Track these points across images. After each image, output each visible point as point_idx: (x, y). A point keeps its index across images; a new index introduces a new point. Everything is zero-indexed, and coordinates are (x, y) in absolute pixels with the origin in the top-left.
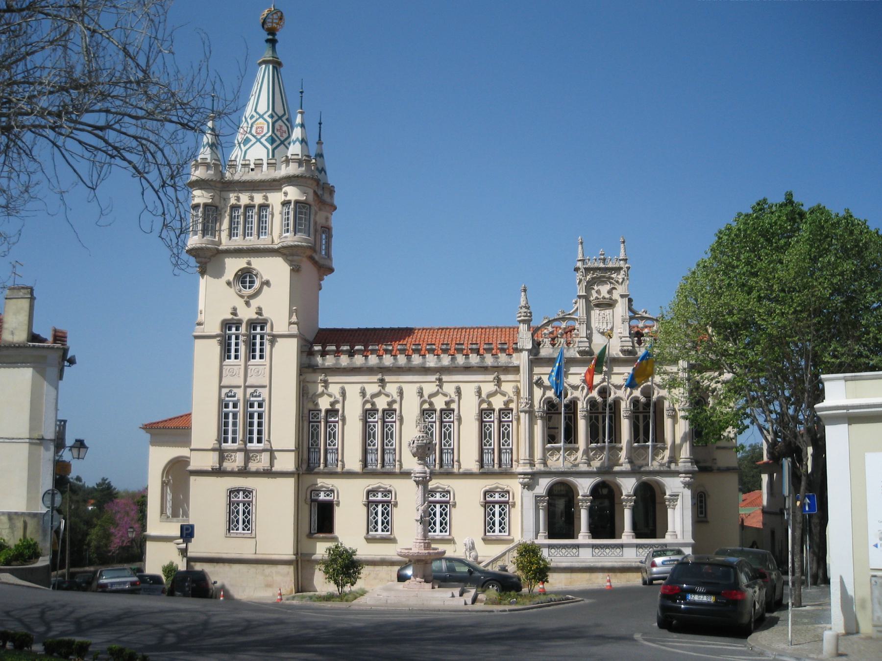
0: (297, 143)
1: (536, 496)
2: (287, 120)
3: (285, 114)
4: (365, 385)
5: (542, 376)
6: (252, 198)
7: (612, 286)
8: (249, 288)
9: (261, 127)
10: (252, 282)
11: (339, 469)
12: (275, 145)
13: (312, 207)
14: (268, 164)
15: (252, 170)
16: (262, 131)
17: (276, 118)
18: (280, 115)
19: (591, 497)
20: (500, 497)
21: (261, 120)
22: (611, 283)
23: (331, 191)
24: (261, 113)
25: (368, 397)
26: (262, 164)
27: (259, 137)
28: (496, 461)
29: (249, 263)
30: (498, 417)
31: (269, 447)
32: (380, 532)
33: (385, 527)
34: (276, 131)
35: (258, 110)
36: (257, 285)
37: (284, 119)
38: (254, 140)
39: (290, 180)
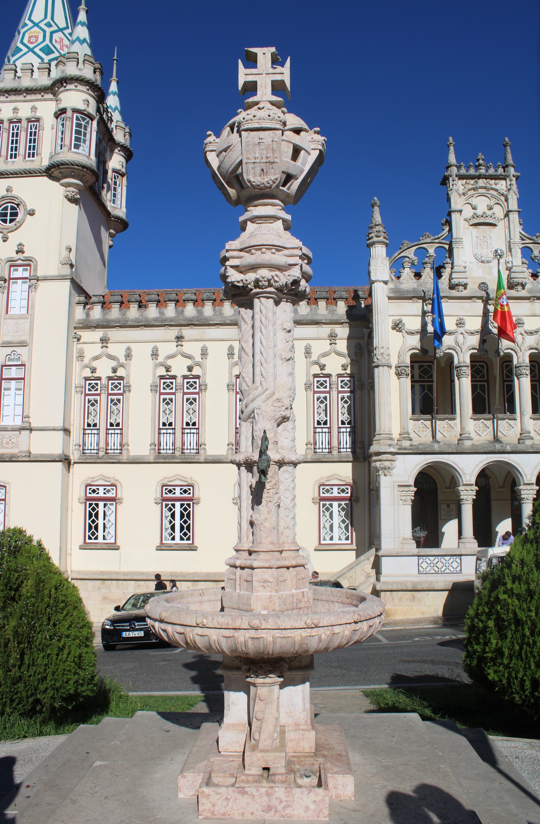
1: (400, 486)
4: (159, 345)
5: (405, 320)
7: (493, 201)
8: (10, 223)
10: (15, 215)
11: (124, 458)
12: (52, 56)
19: (477, 488)
20: (339, 493)
22: (493, 196)
25: (161, 359)
28: (335, 443)
30: (336, 386)
31: (27, 425)
32: (177, 540)
33: (185, 534)
35: (32, 18)
36: (18, 219)
38: (25, 50)
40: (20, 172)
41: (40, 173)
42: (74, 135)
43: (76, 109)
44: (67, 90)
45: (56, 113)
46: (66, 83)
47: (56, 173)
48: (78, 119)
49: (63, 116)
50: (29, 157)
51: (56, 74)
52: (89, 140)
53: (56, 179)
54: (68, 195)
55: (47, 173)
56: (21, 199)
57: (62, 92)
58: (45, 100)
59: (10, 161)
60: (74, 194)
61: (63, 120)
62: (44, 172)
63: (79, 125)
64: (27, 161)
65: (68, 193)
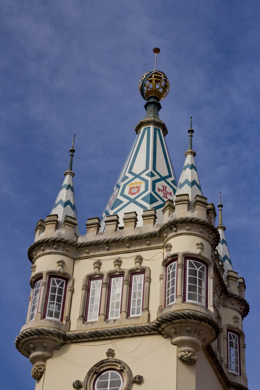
0: (186, 185)
2: (173, 182)
3: (170, 176)
6: (118, 262)
9: (137, 187)
12: (155, 204)
13: (209, 268)
14: (143, 217)
15: (121, 228)
16: (139, 191)
17: (157, 177)
18: (163, 175)
21: (137, 180)
23: (242, 285)
24: (137, 173)
26: (137, 220)
27: (133, 197)
29: (111, 353)
34: (157, 191)
37: (169, 180)
39: (174, 225)
40: (123, 331)
41: (147, 330)
42: (187, 284)
43: (188, 254)
44: (177, 235)
45: (165, 261)
46: (175, 227)
47: (169, 329)
48: (191, 265)
49: (174, 263)
50: (133, 313)
51: (165, 218)
52: (205, 288)
53: (168, 336)
54: (182, 357)
55: (157, 330)
56: (125, 364)
57: (171, 238)
58: (151, 249)
59: (111, 320)
60: (190, 354)
61: (174, 268)
62: (153, 330)
63: (193, 272)
64: (132, 318)
65: (183, 353)
